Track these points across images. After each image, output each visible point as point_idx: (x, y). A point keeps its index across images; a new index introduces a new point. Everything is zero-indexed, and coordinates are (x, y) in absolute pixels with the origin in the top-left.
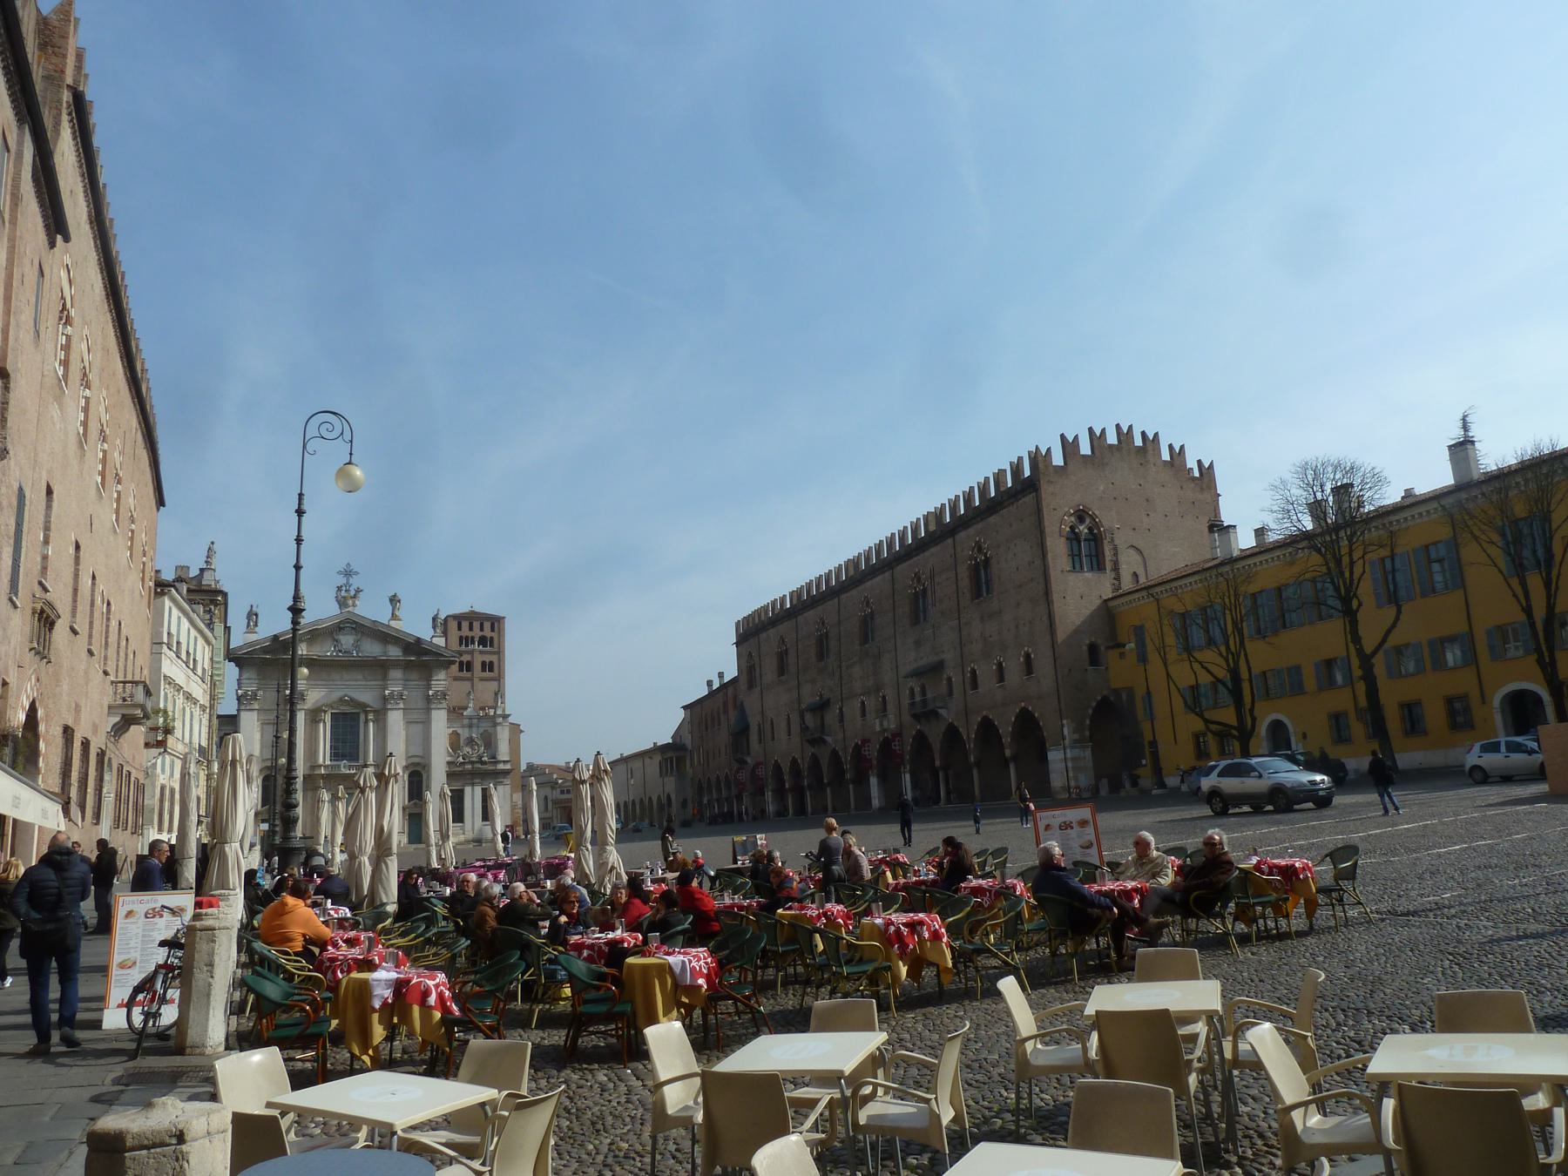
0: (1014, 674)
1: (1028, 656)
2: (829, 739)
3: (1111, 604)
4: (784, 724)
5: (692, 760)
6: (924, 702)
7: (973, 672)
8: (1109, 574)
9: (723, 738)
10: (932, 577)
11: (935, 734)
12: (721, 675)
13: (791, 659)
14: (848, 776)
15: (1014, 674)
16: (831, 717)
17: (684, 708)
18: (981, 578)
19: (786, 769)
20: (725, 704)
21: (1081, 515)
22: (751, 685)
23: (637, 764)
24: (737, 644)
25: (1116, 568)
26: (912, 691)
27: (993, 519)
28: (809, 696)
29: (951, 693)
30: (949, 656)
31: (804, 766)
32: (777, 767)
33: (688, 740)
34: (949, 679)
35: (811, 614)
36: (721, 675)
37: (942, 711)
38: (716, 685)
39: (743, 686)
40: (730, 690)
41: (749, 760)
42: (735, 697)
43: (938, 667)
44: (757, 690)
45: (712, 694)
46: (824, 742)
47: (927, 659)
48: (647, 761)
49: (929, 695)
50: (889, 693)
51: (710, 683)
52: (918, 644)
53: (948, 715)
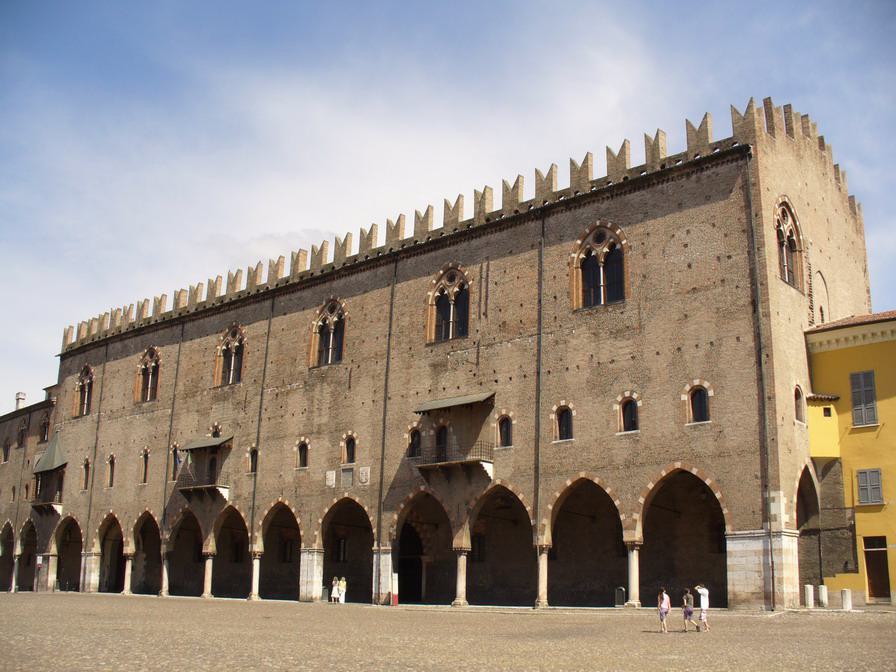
0: (664, 414)
1: (699, 396)
2: (225, 493)
3: (814, 338)
7: (564, 415)
8: (807, 299)
10: (484, 279)
15: (664, 414)
18: (604, 279)
21: (786, 208)
24: (63, 357)
25: (810, 295)
27: (635, 197)
28: (193, 432)
29: (506, 440)
34: (505, 423)
37: (489, 468)
40: (37, 417)
43: (487, 405)
46: (214, 494)
47: (458, 391)
52: (438, 368)
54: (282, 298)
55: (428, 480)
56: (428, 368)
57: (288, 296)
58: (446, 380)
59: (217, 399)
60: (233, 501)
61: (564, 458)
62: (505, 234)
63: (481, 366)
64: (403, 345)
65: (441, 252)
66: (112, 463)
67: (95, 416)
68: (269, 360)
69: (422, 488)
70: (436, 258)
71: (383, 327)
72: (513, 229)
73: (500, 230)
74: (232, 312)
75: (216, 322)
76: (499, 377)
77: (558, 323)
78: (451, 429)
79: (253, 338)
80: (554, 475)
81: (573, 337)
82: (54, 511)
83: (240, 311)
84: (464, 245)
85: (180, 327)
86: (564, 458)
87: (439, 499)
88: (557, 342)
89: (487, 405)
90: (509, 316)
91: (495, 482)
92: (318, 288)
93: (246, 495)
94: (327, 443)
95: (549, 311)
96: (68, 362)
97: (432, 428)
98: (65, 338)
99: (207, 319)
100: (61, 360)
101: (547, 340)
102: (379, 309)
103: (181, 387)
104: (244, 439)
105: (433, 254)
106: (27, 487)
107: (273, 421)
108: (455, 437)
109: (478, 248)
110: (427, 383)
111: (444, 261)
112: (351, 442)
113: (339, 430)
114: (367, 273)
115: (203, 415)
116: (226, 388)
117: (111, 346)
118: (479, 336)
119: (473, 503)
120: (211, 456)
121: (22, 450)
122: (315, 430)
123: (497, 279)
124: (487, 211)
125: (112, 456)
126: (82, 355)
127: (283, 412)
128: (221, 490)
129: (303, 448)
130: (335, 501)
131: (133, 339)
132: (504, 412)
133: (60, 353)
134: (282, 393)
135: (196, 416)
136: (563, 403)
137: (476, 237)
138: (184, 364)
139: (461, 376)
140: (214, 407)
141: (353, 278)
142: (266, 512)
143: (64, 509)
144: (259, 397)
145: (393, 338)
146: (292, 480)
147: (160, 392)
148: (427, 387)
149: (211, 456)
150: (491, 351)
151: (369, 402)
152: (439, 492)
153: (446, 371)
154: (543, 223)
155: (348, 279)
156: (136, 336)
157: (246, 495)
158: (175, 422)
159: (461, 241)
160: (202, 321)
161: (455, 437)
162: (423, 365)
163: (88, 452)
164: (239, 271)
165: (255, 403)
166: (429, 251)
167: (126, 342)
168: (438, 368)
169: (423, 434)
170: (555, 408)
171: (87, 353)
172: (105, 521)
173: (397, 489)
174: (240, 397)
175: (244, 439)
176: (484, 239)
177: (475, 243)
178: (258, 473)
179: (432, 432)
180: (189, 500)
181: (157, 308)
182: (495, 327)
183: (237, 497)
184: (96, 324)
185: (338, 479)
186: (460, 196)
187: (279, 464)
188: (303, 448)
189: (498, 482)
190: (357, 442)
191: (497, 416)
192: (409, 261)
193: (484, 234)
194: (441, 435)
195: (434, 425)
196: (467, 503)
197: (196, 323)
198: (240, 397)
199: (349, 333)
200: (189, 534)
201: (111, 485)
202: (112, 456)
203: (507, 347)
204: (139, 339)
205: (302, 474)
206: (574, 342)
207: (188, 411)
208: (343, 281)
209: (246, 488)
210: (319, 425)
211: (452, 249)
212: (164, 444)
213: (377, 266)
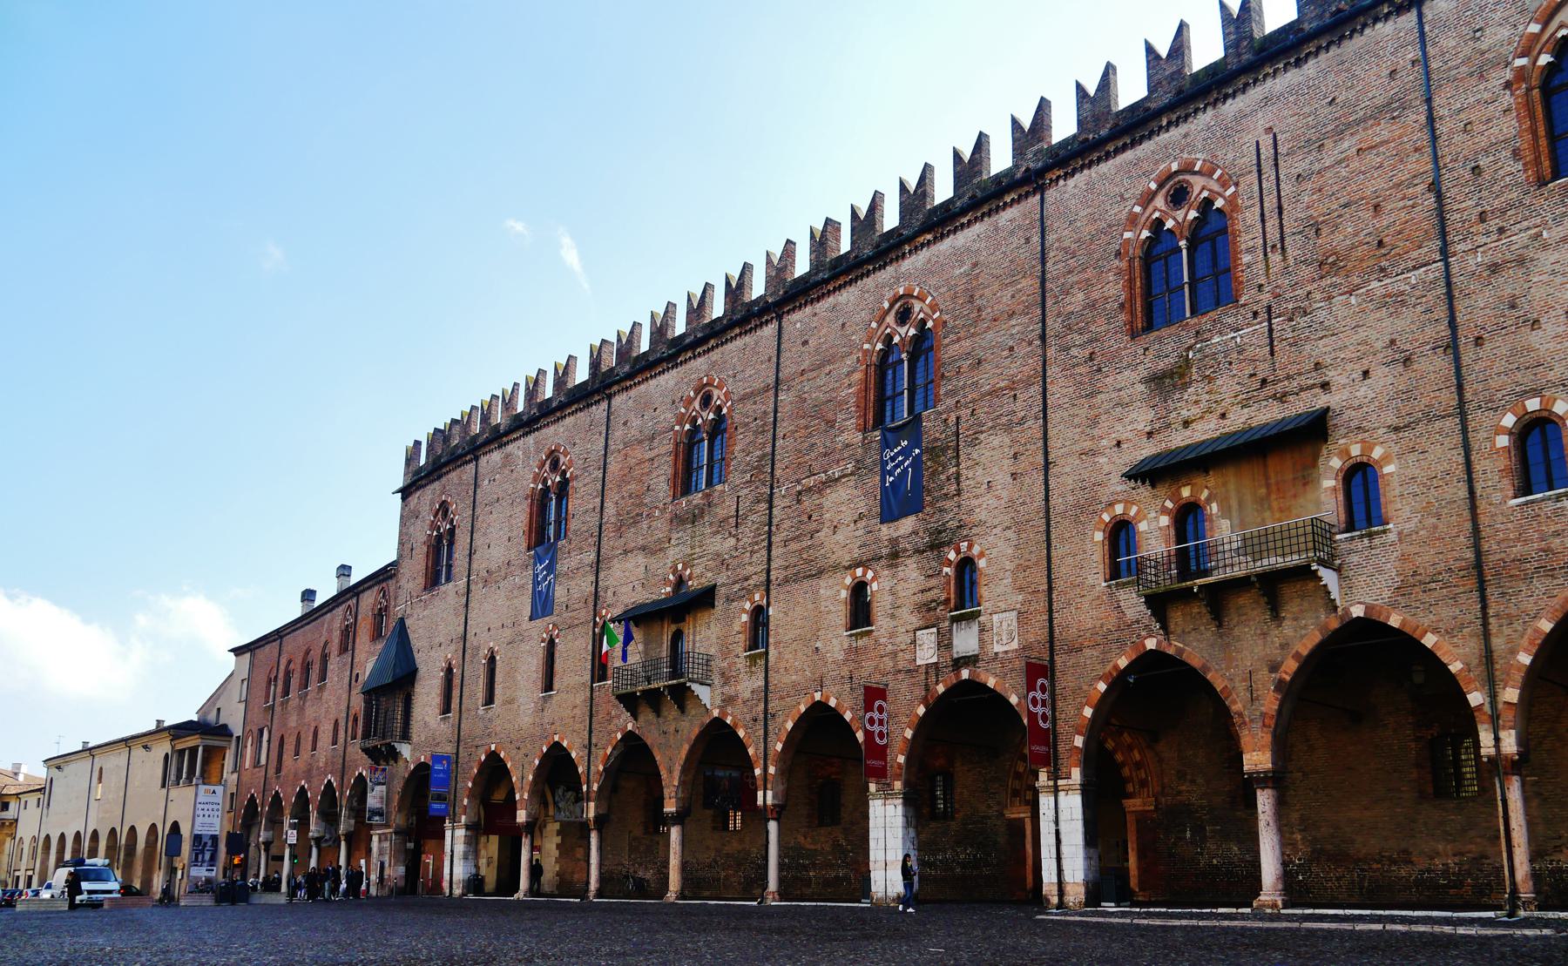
2: (702, 692)
4: (532, 665)
5: (239, 756)
6: (1188, 560)
9: (335, 700)
11: (1252, 665)
12: (344, 571)
13: (581, 502)
14: (766, 797)
16: (708, 637)
17: (238, 651)
19: (523, 774)
20: (348, 634)
22: (435, 576)
23: (114, 762)
26: (1121, 533)
30: (1361, 398)
31: (592, 768)
32: (495, 770)
33: (234, 718)
34: (1360, 477)
35: (666, 383)
36: (344, 571)
37: (1328, 577)
38: (327, 590)
39: (412, 578)
40: (368, 599)
41: (405, 750)
42: (380, 614)
43: (1312, 432)
44: (450, 591)
45: (310, 617)
48: (138, 752)
49: (1223, 530)
50: (997, 556)
51: (308, 595)
53: (1364, 586)
54: (796, 316)
55: (1165, 627)
56: (1141, 387)
57: (808, 310)
58: (1187, 403)
59: (678, 520)
60: (721, 708)
61: (1557, 534)
62: (1310, 68)
63: (1281, 358)
64: (1074, 352)
65: (1147, 147)
66: (492, 660)
67: (462, 582)
68: (780, 432)
69: (1151, 644)
70: (1136, 163)
71: (1022, 326)
72: (1334, 50)
73: (1298, 63)
74: (700, 360)
75: (672, 383)
76: (1331, 375)
77: (1494, 224)
78: (1214, 506)
79: (743, 399)
80: (1527, 578)
81: (1545, 247)
82: (394, 755)
83: (715, 355)
84: (1206, 118)
85: (604, 405)
86: (1557, 534)
87: (1196, 662)
88: (1494, 268)
89: (1312, 432)
90: (1338, 240)
91: (1347, 611)
92: (868, 282)
93: (747, 695)
94: (912, 572)
95: (1462, 206)
96: (413, 500)
97: (1164, 511)
98: (408, 461)
99: (652, 382)
100: (403, 499)
101: (1468, 261)
102: (1011, 290)
103: (610, 509)
104: (737, 586)
105: (1129, 155)
106: (355, 720)
107: (794, 546)
108: (1225, 524)
109: (1241, 116)
110: (1142, 417)
111: (1157, 163)
112: (966, 566)
113: (936, 545)
114: (978, 228)
115: (653, 553)
116: (697, 498)
117: (483, 460)
118: (1266, 298)
119: (1291, 666)
120: (674, 628)
121: (347, 657)
122: (885, 551)
123: (1301, 167)
124: (1257, 35)
125: (491, 650)
126: (436, 485)
127: (813, 526)
128: (695, 687)
129: (859, 589)
130: (941, 689)
131: (520, 442)
132: (1355, 450)
133: (400, 485)
134: (810, 489)
135: (641, 559)
136: (1533, 404)
137: (1234, 96)
138: (614, 466)
139: (1227, 385)
140: (675, 536)
141: (945, 245)
142: (789, 725)
143: (413, 750)
144: (764, 506)
145: (1051, 341)
146: (841, 656)
147: (574, 525)
148: (1142, 426)
149: (674, 628)
150: (1302, 321)
151: (1002, 479)
152: (1193, 644)
153: (1186, 386)
154: (1420, 16)
155: (934, 249)
156: (526, 434)
157: (747, 695)
158: (602, 575)
159: (1196, 111)
160: (643, 387)
161: (1225, 524)
162: (1129, 380)
163: (453, 647)
164: (708, 287)
165: (757, 517)
166: (1117, 151)
167: (510, 448)
168: (1166, 382)
169: (1142, 527)
170: (1509, 420)
171: (444, 479)
172: (482, 766)
173: (1087, 652)
174: (726, 509)
175: (737, 586)
176: (1256, 93)
177: (1231, 107)
178: (772, 652)
179: (1165, 520)
180: (635, 716)
181: (560, 382)
182: (1306, 272)
183: (729, 700)
184: (457, 429)
185: (944, 643)
186: (1182, 28)
187: (811, 625)
188: (859, 589)
189: (1357, 611)
190: (982, 563)
191: (1336, 463)
192: (1071, 182)
193: (1256, 81)
194: (1187, 518)
195: (1169, 504)
196: (1274, 668)
197: (633, 393)
198: (726, 509)
199: (950, 350)
200: (633, 758)
201: (490, 699)
202: (491, 650)
203: (1348, 304)
204: (530, 439)
205: (860, 643)
206: (1548, 259)
207: (626, 552)
208: (924, 254)
209: (748, 685)
210: (894, 542)
211: (1175, 133)
212: (585, 614)
213: (997, 210)
